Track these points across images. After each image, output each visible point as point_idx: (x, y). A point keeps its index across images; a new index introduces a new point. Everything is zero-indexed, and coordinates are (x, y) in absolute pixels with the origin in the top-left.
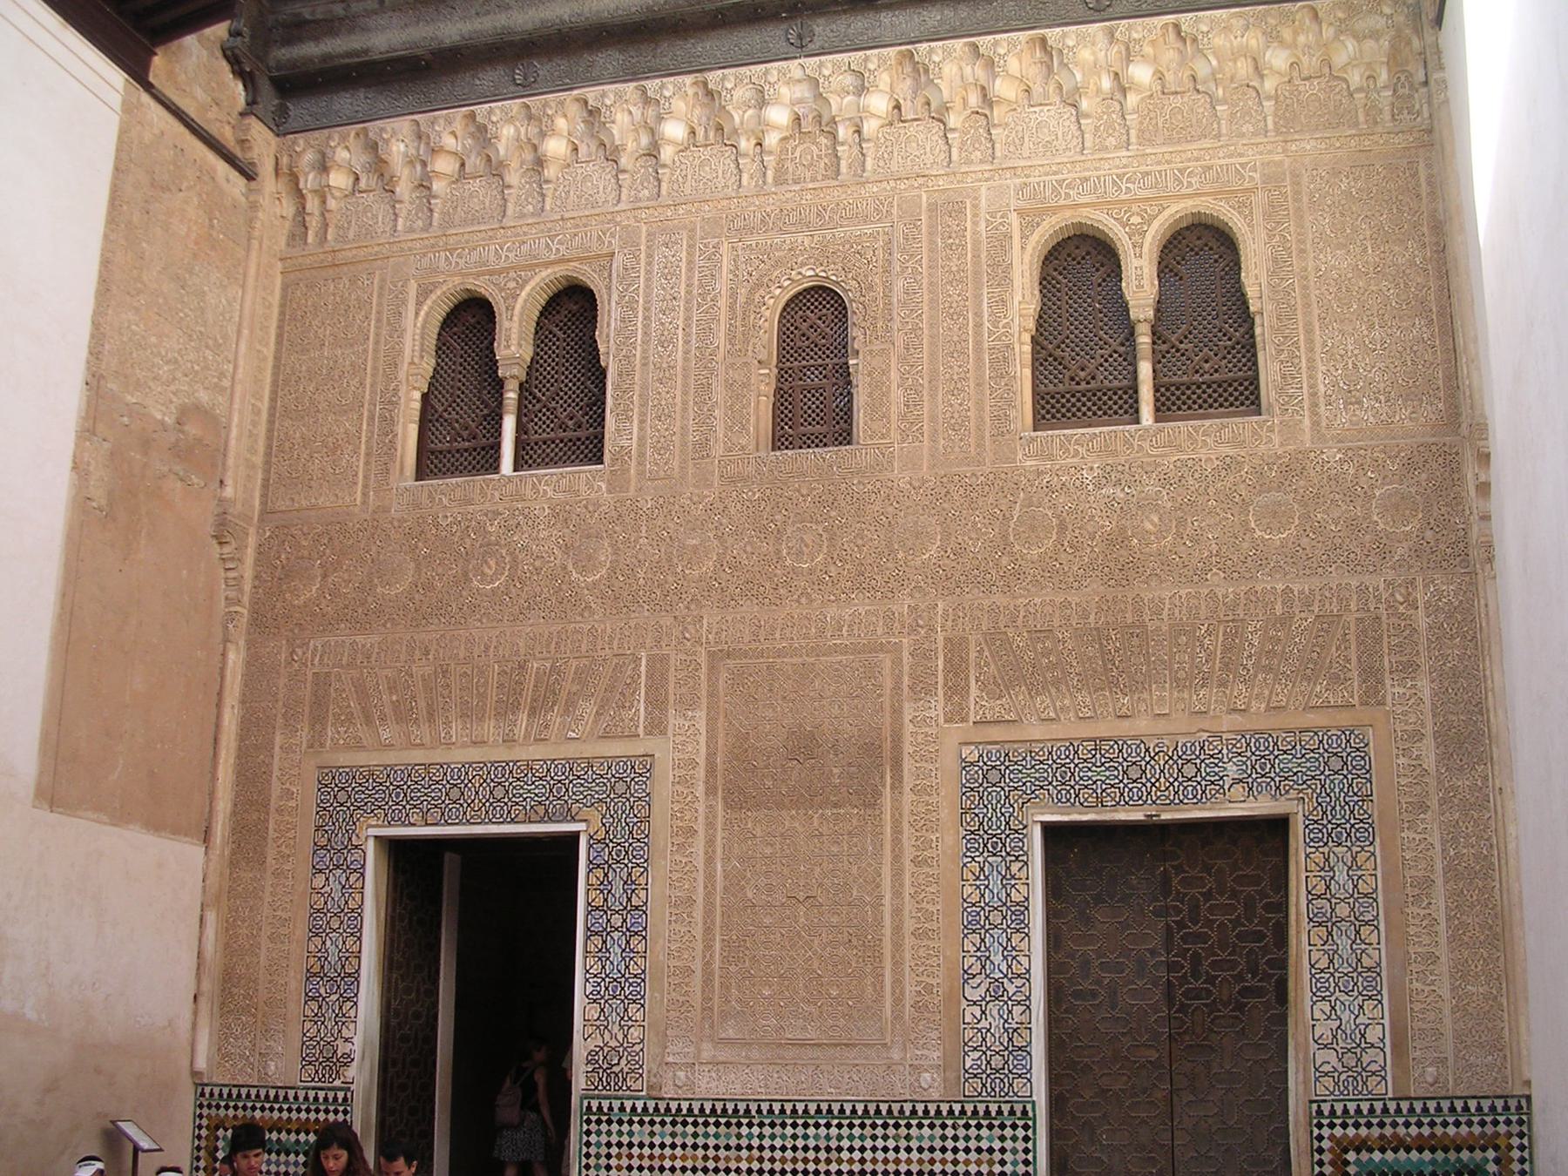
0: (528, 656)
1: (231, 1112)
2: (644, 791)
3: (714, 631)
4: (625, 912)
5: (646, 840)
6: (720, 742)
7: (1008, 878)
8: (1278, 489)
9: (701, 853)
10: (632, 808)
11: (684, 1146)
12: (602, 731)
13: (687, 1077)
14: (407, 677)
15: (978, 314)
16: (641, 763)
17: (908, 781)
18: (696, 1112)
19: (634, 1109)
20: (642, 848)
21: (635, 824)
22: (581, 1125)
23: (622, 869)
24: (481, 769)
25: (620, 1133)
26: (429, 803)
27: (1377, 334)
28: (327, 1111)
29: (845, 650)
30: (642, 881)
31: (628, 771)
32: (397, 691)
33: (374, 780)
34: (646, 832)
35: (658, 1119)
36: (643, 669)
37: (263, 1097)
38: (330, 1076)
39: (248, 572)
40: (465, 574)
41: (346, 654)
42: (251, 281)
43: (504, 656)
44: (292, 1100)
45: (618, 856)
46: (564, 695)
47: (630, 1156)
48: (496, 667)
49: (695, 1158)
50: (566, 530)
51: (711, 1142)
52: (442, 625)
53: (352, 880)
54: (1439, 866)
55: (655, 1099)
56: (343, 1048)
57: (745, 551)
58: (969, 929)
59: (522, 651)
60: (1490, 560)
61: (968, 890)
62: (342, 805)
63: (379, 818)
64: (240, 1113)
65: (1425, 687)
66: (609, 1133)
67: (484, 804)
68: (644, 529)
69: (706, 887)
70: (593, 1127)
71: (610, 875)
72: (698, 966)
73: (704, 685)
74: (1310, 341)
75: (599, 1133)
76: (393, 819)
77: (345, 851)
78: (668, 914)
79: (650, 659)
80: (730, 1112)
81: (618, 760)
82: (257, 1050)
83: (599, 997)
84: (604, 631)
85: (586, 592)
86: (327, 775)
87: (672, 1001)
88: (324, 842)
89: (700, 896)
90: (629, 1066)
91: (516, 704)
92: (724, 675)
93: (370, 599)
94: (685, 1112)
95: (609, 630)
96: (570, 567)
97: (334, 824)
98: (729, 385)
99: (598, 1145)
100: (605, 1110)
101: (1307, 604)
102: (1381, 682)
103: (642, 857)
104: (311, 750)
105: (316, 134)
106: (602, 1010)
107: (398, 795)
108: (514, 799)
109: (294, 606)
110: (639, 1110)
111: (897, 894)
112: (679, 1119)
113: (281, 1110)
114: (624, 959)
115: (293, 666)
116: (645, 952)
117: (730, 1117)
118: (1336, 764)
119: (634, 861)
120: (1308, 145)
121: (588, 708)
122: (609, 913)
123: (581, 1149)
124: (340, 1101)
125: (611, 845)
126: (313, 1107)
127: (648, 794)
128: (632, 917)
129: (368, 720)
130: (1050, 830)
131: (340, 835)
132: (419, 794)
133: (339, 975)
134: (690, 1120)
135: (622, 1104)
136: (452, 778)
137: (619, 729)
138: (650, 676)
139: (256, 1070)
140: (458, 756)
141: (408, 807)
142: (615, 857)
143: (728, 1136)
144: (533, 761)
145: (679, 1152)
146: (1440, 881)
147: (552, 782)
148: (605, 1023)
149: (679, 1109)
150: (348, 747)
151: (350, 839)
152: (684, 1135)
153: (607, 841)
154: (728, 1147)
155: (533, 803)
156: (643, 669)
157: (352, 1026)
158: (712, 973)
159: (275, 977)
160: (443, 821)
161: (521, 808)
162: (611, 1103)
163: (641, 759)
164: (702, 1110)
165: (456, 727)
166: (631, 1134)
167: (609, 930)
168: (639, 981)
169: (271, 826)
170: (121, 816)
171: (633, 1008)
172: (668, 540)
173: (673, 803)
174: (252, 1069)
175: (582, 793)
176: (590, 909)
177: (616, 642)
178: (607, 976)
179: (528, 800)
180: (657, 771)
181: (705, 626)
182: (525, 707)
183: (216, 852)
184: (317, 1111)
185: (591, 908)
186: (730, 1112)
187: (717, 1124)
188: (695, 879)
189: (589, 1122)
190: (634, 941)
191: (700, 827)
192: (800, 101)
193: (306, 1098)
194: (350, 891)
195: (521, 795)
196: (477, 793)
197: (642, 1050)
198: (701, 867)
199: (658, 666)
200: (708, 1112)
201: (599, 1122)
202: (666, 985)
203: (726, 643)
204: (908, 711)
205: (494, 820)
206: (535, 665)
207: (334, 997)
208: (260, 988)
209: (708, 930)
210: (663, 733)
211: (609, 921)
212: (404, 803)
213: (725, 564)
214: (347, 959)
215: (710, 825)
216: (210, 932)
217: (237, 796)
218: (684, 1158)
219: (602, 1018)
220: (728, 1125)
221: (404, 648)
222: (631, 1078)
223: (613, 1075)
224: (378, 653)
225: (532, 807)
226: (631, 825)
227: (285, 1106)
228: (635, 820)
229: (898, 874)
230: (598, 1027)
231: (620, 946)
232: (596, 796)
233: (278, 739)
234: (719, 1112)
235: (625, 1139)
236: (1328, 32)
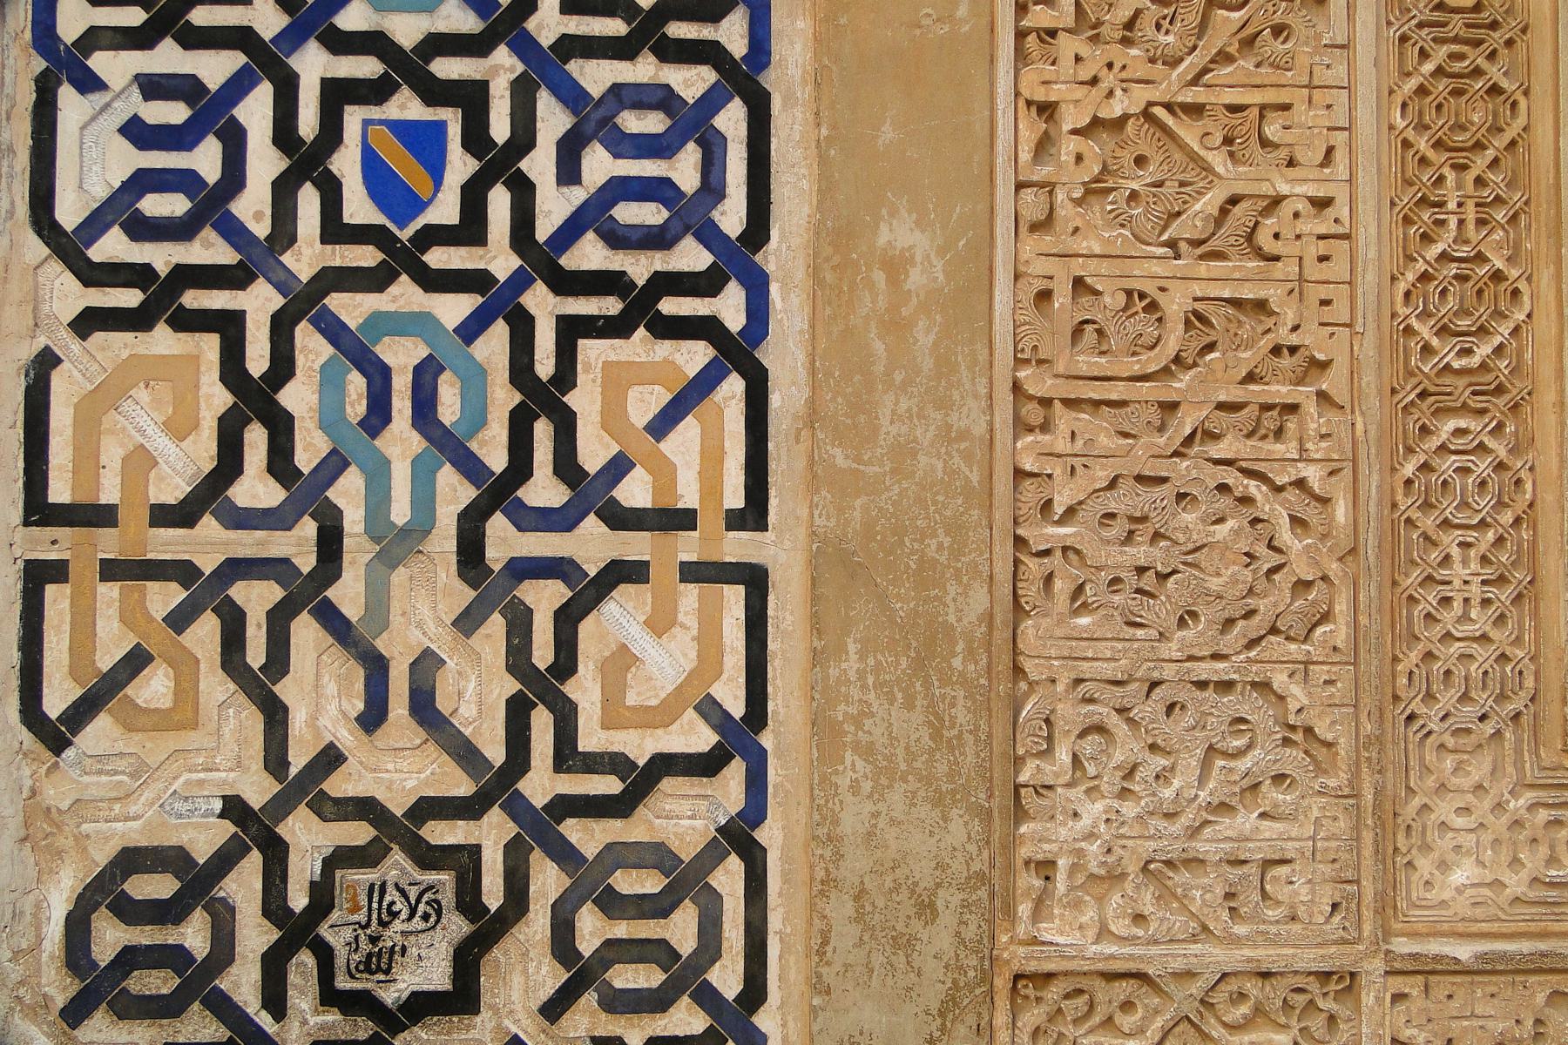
83: (210, 250)
168: (692, 82)
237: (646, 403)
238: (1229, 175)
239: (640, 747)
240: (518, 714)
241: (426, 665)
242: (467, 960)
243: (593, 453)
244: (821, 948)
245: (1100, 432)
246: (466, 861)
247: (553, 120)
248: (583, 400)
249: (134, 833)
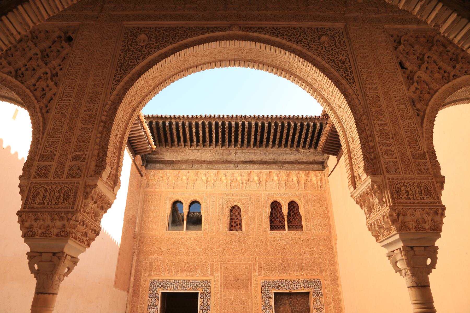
7: (269, 301)
8: (306, 242)
15: (262, 212)
17: (253, 286)
27: (320, 220)
29: (242, 264)
39: (138, 244)
42: (141, 194)
53: (156, 299)
54: (332, 300)
58: (263, 310)
60: (337, 254)
61: (263, 303)
65: (328, 273)
74: (310, 220)
79: (210, 263)
89: (219, 304)
92: (223, 267)
98: (223, 220)
101: (311, 260)
102: (322, 272)
105: (153, 170)
111: (252, 304)
118: (316, 284)
120: (309, 192)
121: (199, 271)
130: (275, 293)
138: (210, 266)
140: (177, 278)
146: (332, 302)
170: (121, 289)
183: (129, 294)
191: (219, 292)
192: (235, 176)
199: (212, 264)
204: (253, 274)
216: (128, 309)
229: (252, 300)
233: (142, 274)
236: (313, 175)
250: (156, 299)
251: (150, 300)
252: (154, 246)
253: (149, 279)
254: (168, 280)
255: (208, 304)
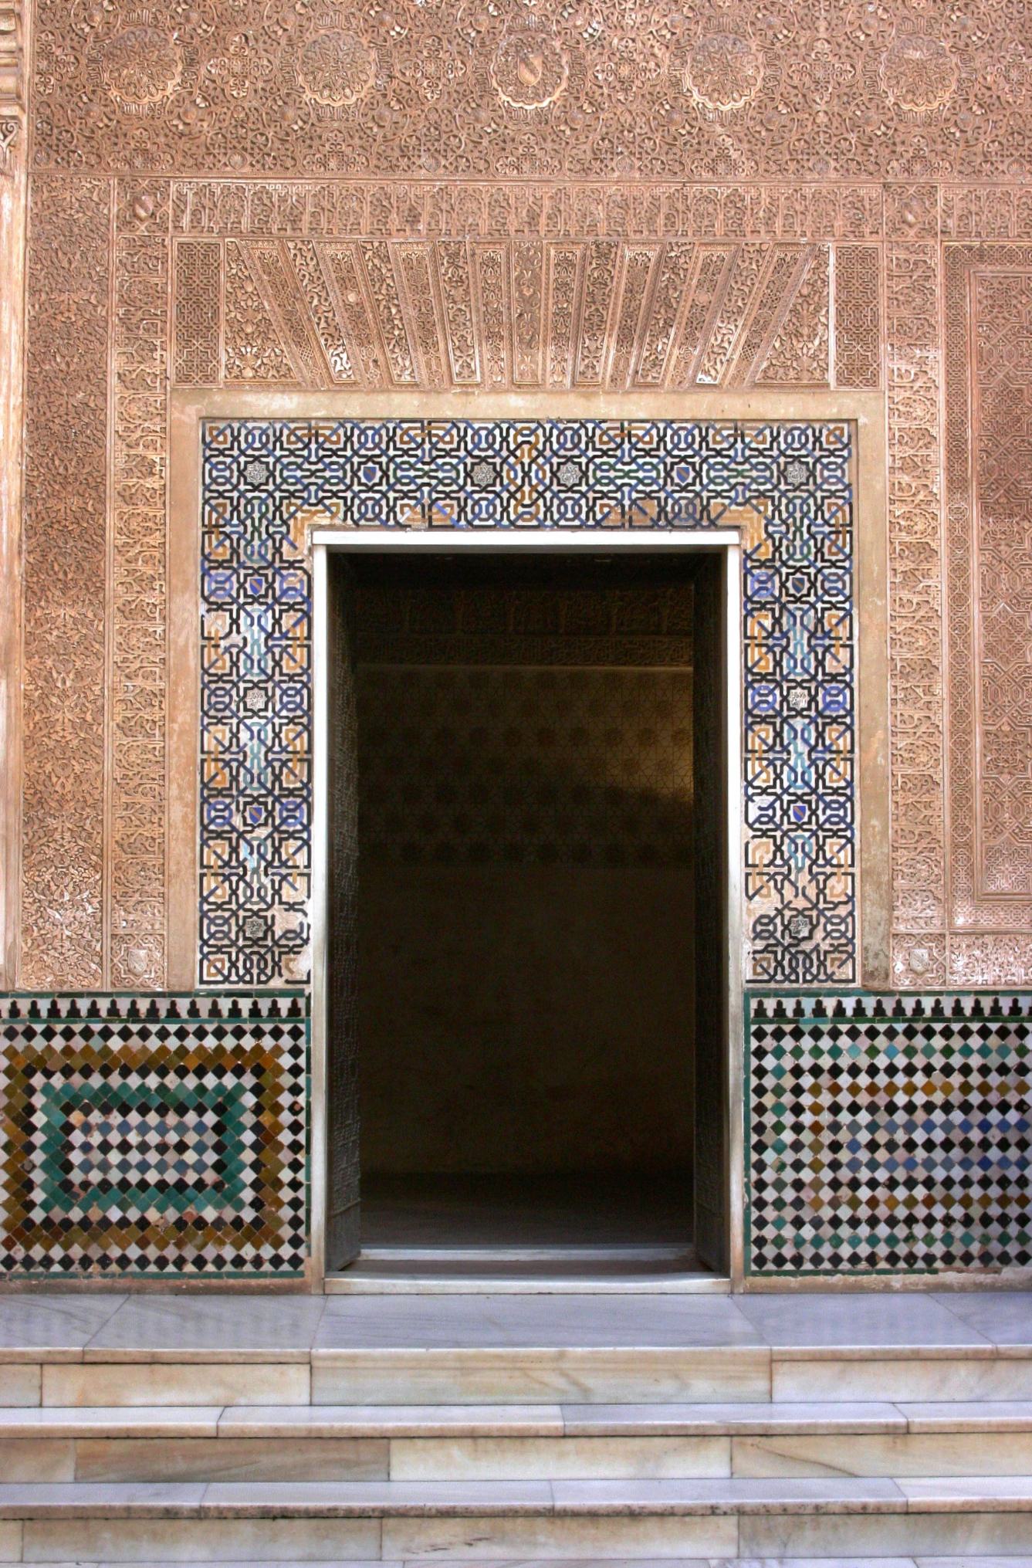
0: (615, 238)
1: (58, 1043)
2: (840, 480)
3: (956, 212)
4: (813, 685)
5: (847, 564)
6: (972, 403)
9: (945, 589)
10: (819, 508)
11: (928, 1070)
12: (759, 375)
13: (932, 958)
14: (376, 261)
16: (830, 432)
18: (948, 1012)
19: (840, 1010)
20: (840, 578)
21: (826, 536)
22: (747, 1042)
23: (805, 612)
24: (533, 432)
25: (817, 1052)
26: (434, 489)
28: (258, 1033)
30: (842, 632)
31: (810, 446)
32: (355, 286)
33: (320, 446)
34: (847, 550)
35: (882, 1027)
36: (831, 271)
37: (124, 1013)
38: (262, 971)
40: (483, 81)
41: (248, 212)
43: (567, 234)
44: (184, 1015)
45: (798, 590)
46: (684, 311)
47: (835, 1090)
48: (553, 253)
49: (947, 1089)
50: (677, 16)
51: (975, 1061)
52: (442, 171)
53: (287, 621)
55: (876, 993)
56: (284, 921)
57: (1007, 79)
59: (602, 228)
62: (256, 488)
63: (334, 515)
64: (78, 1043)
66: (797, 1052)
67: (541, 495)
68: (822, 25)
69: (953, 645)
70: (769, 1043)
71: (784, 620)
72: (943, 774)
73: (941, 306)
75: (779, 1053)
76: (363, 516)
77: (270, 572)
78: (890, 689)
80: (1006, 1011)
81: (789, 426)
82: (107, 928)
83: (771, 826)
84: (756, 201)
85: (719, 129)
86: (222, 432)
87: (900, 833)
88: (222, 553)
90: (828, 941)
91: (596, 319)
93: (291, 113)
94: (928, 1013)
95: (765, 199)
96: (688, 82)
97: (242, 522)
99: (779, 1072)
100: (790, 1013)
103: (840, 592)
104: (187, 386)
106: (778, 848)
107: (370, 474)
108: (598, 488)
109: (128, 116)
110: (849, 1013)
112: (920, 1026)
113: (163, 1035)
114: (813, 762)
115: (133, 229)
116: (852, 751)
117: (1005, 1020)
119: (826, 598)
121: (733, 335)
122: (785, 685)
123: (747, 1081)
124: (284, 1013)
125: (784, 570)
126: (229, 1027)
127: (848, 487)
128: (827, 693)
129: (299, 336)
131: (256, 543)
132: (412, 473)
133: (270, 792)
134: (938, 1027)
135: (819, 1003)
136: (476, 446)
137: (792, 374)
139: (107, 965)
141: (391, 495)
142: (792, 591)
143: (1003, 1052)
144: (631, 421)
145: (919, 1079)
147: (669, 460)
148: (785, 870)
149: (918, 1010)
150: (261, 384)
151: (278, 550)
152: (929, 1051)
153: (778, 564)
154: (1003, 1070)
155: (634, 495)
156: (831, 271)
157: (301, 882)
158: (968, 788)
159: (139, 798)
160: (463, 522)
161: (613, 503)
162: (798, 1003)
163: (832, 426)
164: (958, 1010)
165: (480, 356)
166: (835, 1052)
167: (785, 713)
168: (842, 799)
169: (111, 520)
171: (832, 845)
172: (867, 48)
173: (892, 502)
174: (100, 965)
175: (726, 480)
176: (750, 678)
177: (779, 223)
178: (785, 791)
179: (740, 488)
180: (865, 443)
181: (941, 203)
182: (612, 329)
184: (239, 1033)
185: (752, 677)
186: (1006, 1011)
187: (984, 1033)
188: (935, 632)
189: (760, 1035)
190: (831, 733)
191: (941, 544)
193: (215, 1012)
194: (284, 643)
195: (612, 481)
196: (526, 474)
197: (851, 914)
198: (945, 612)
200: (968, 1012)
201: (778, 1035)
202: (891, 806)
203: (979, 234)
205: (562, 523)
206: (627, 253)
207: (262, 832)
208: (107, 817)
209: (960, 716)
210: (872, 382)
211: (785, 699)
212: (384, 488)
213: (972, 98)
214: (284, 763)
215: (958, 542)
217: (33, 464)
218: (929, 1089)
219: (779, 862)
220: (1003, 1033)
221: (367, 209)
222: (833, 960)
223: (801, 957)
224: (313, 214)
225: (633, 502)
226: (819, 537)
227: (173, 1028)
228: (827, 529)
230: (772, 877)
231: (806, 741)
232: (754, 487)
233: (115, 363)
234: (987, 1012)
235: (826, 1062)
237: (835, 848)
238: (926, 812)
239: (836, 900)
240: (818, 896)
241: (804, 888)
242: (811, 932)
243: (828, 856)
244: (862, 930)
245: (905, 852)
246: (810, 917)
247: (821, 806)
248: (827, 848)
249: (762, 912)
250: (287, 621)
251: (218, 623)
252: (209, 67)
253: (187, 415)
254: (392, 430)
255: (831, 666)
